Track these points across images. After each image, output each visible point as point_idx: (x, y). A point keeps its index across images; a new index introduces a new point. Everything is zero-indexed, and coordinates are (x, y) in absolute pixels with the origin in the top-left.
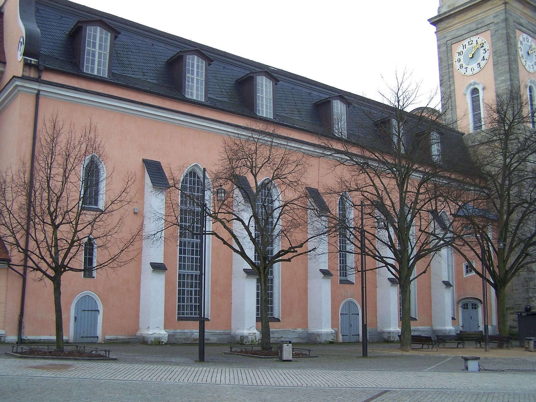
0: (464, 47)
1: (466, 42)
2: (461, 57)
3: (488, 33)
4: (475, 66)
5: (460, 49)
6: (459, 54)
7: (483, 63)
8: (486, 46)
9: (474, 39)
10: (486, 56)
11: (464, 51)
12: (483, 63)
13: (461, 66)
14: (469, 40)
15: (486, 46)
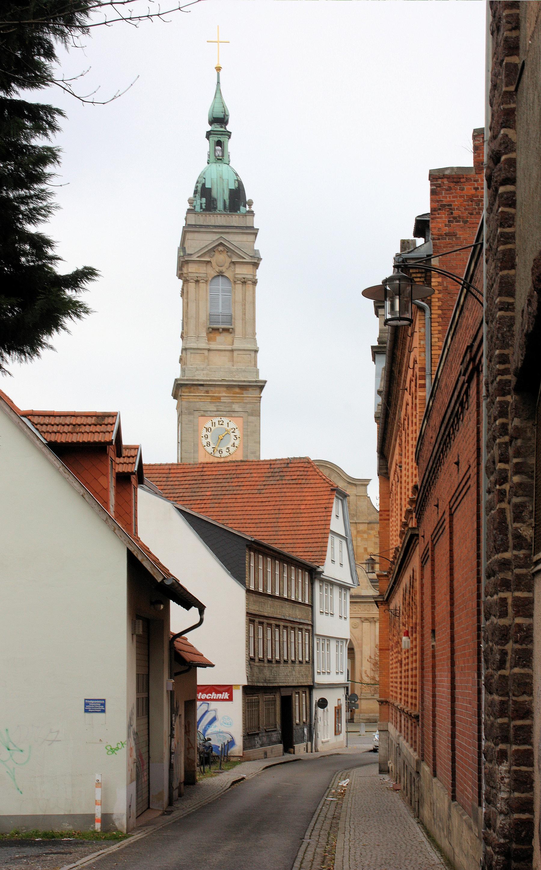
0: (213, 424)
1: (216, 420)
2: (208, 433)
3: (240, 420)
4: (224, 449)
5: (209, 425)
6: (207, 430)
7: (232, 450)
8: (237, 433)
9: (226, 420)
10: (237, 443)
11: (213, 428)
12: (232, 450)
13: (208, 444)
14: (218, 419)
15: (237, 433)
